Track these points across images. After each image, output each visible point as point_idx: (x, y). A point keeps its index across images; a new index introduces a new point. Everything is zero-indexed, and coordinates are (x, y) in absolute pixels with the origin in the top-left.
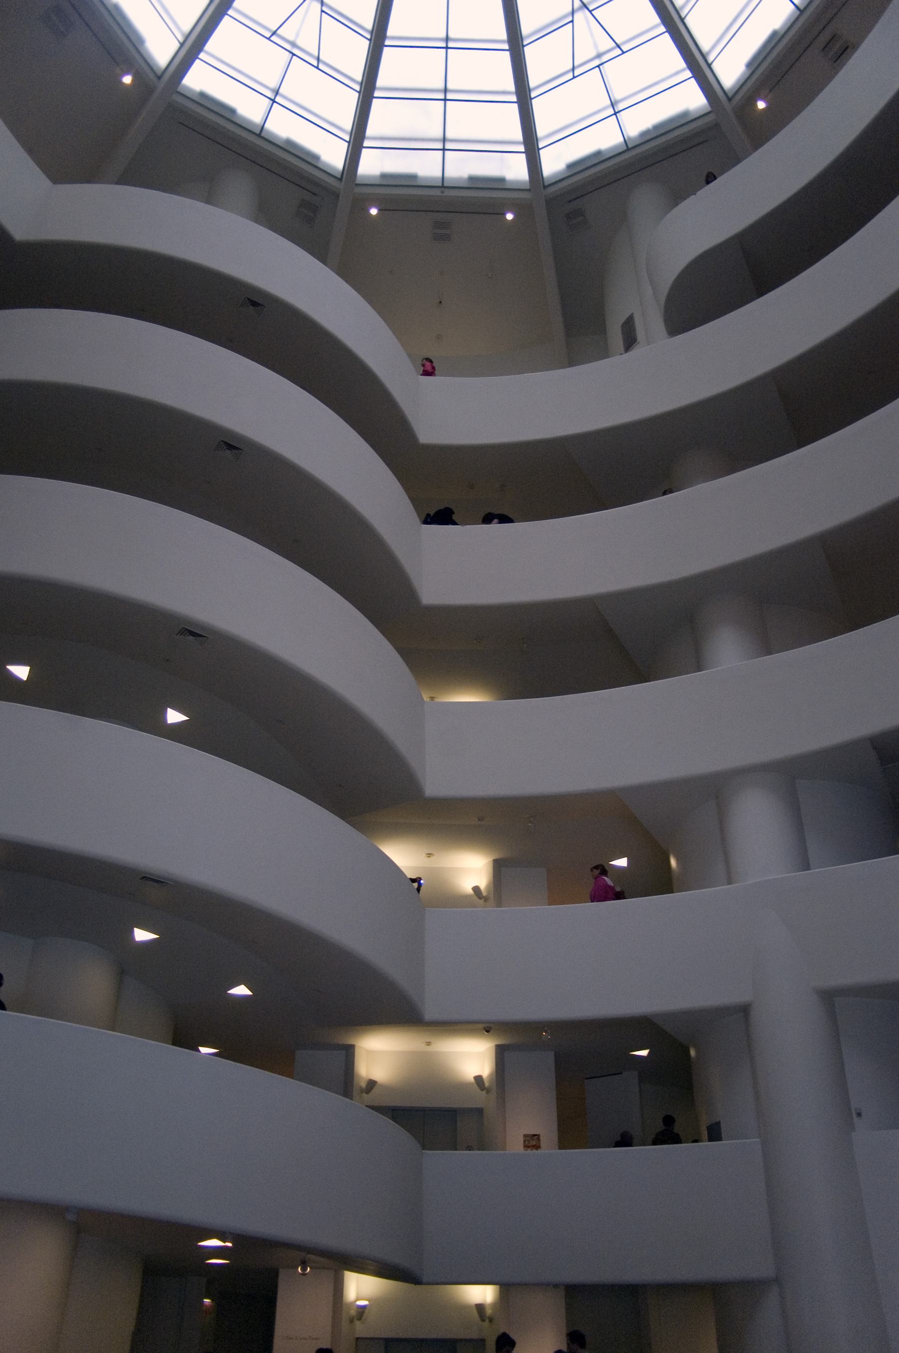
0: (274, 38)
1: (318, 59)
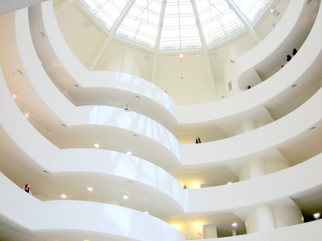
0: (137, 19)
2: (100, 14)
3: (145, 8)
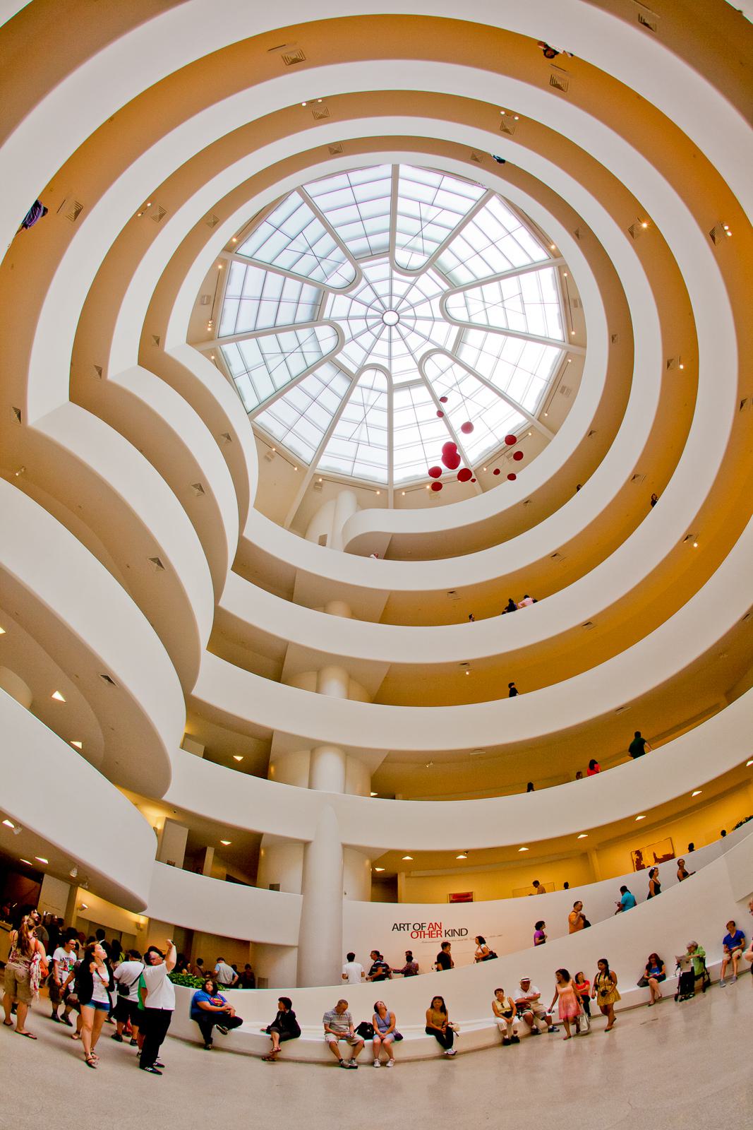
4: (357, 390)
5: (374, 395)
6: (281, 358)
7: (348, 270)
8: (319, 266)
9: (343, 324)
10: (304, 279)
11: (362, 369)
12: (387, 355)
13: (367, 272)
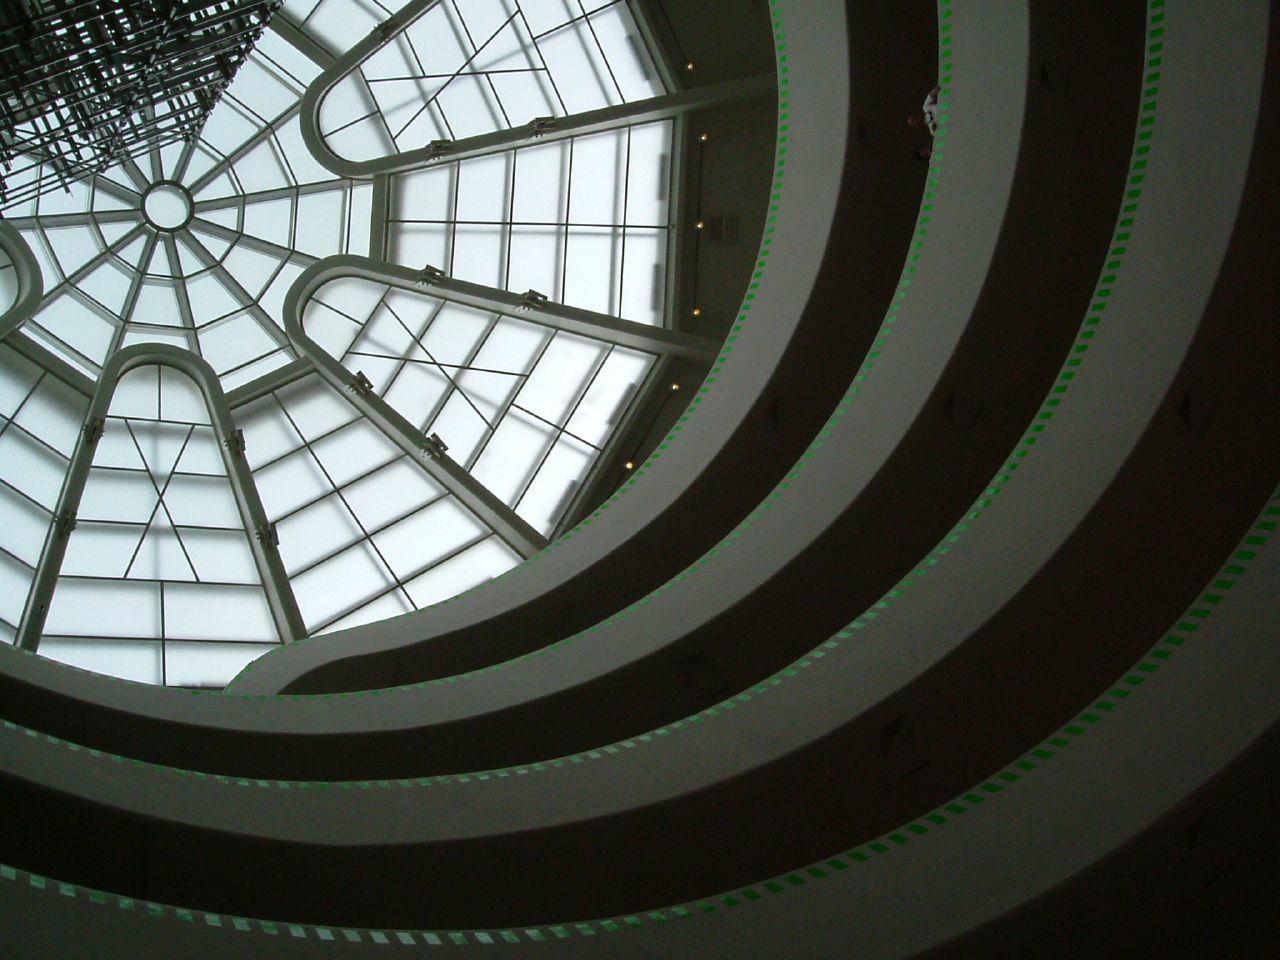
1: (511, 19)
2: (646, 206)
3: (474, 73)
4: (407, 143)
5: (385, 96)
6: (469, 380)
7: (132, 399)
8: (176, 470)
9: (274, 305)
10: (242, 479)
11: (347, 172)
12: (264, 146)
13: (99, 354)
